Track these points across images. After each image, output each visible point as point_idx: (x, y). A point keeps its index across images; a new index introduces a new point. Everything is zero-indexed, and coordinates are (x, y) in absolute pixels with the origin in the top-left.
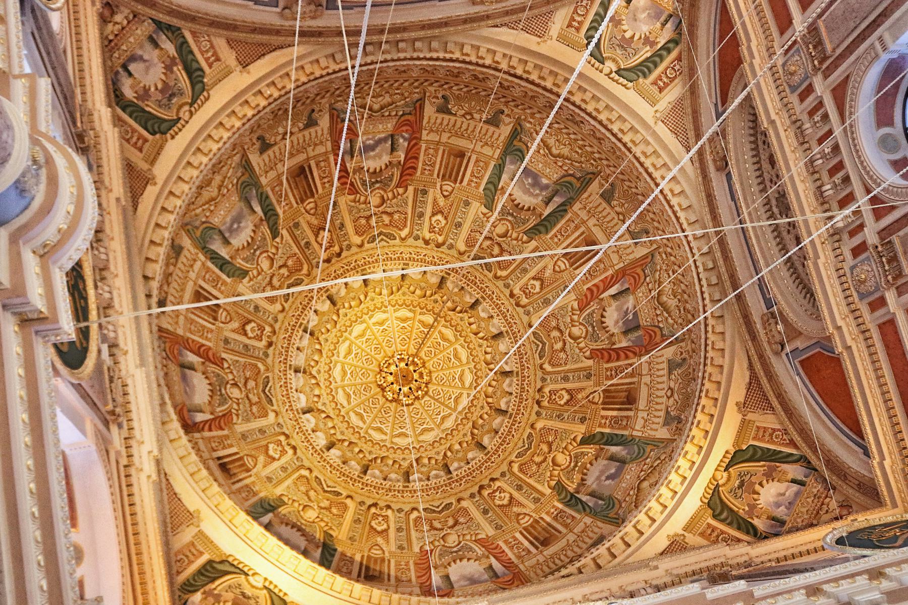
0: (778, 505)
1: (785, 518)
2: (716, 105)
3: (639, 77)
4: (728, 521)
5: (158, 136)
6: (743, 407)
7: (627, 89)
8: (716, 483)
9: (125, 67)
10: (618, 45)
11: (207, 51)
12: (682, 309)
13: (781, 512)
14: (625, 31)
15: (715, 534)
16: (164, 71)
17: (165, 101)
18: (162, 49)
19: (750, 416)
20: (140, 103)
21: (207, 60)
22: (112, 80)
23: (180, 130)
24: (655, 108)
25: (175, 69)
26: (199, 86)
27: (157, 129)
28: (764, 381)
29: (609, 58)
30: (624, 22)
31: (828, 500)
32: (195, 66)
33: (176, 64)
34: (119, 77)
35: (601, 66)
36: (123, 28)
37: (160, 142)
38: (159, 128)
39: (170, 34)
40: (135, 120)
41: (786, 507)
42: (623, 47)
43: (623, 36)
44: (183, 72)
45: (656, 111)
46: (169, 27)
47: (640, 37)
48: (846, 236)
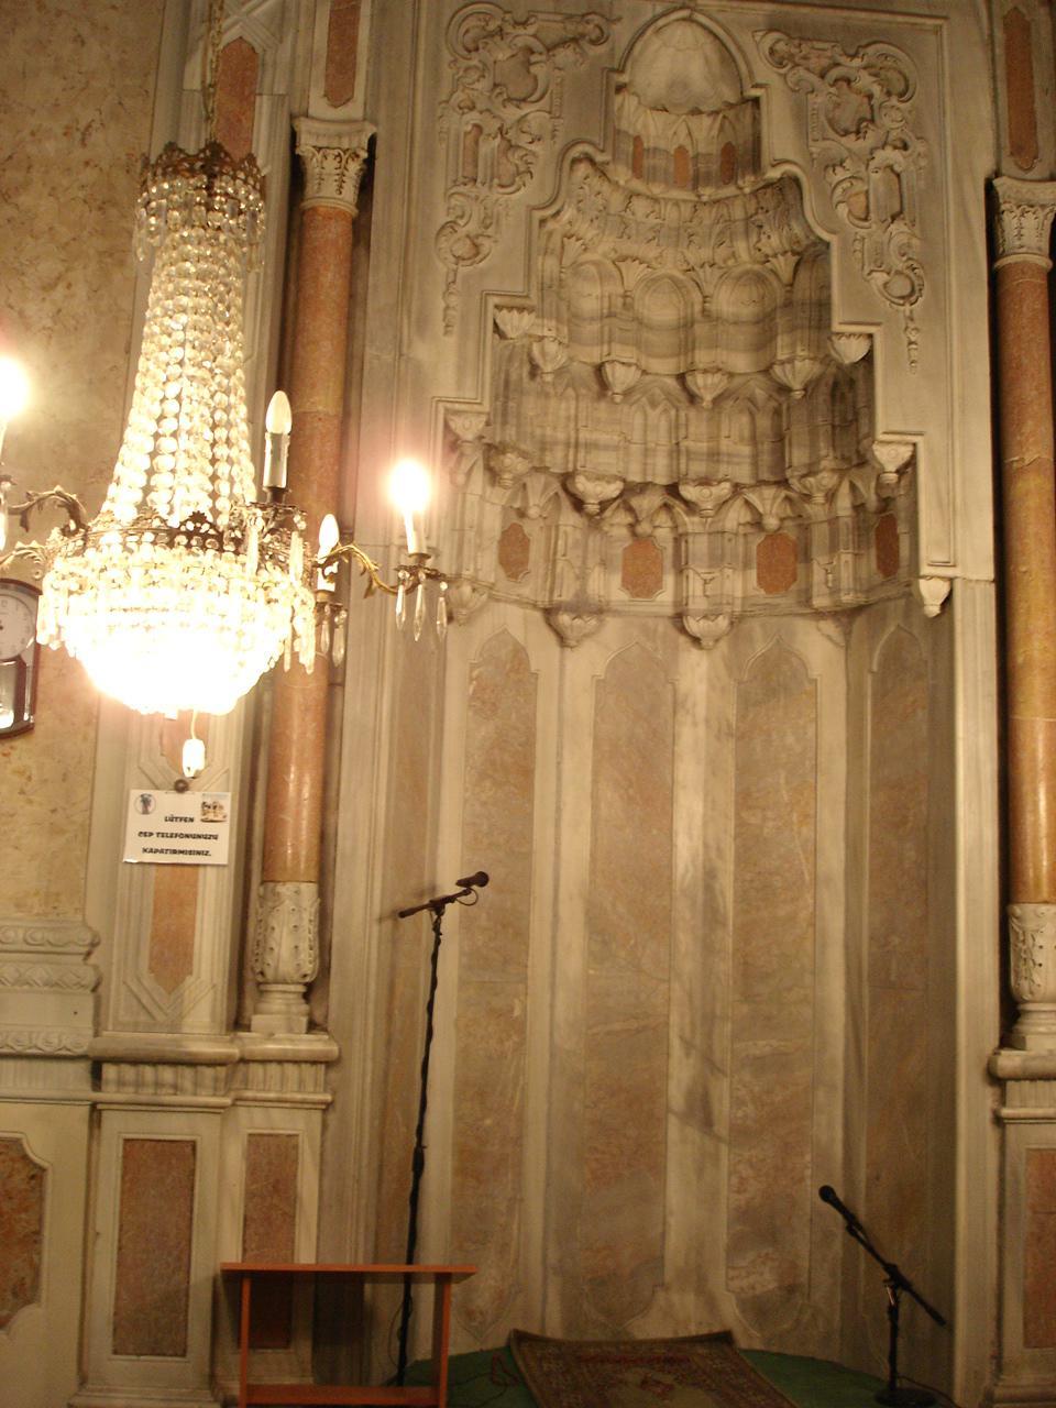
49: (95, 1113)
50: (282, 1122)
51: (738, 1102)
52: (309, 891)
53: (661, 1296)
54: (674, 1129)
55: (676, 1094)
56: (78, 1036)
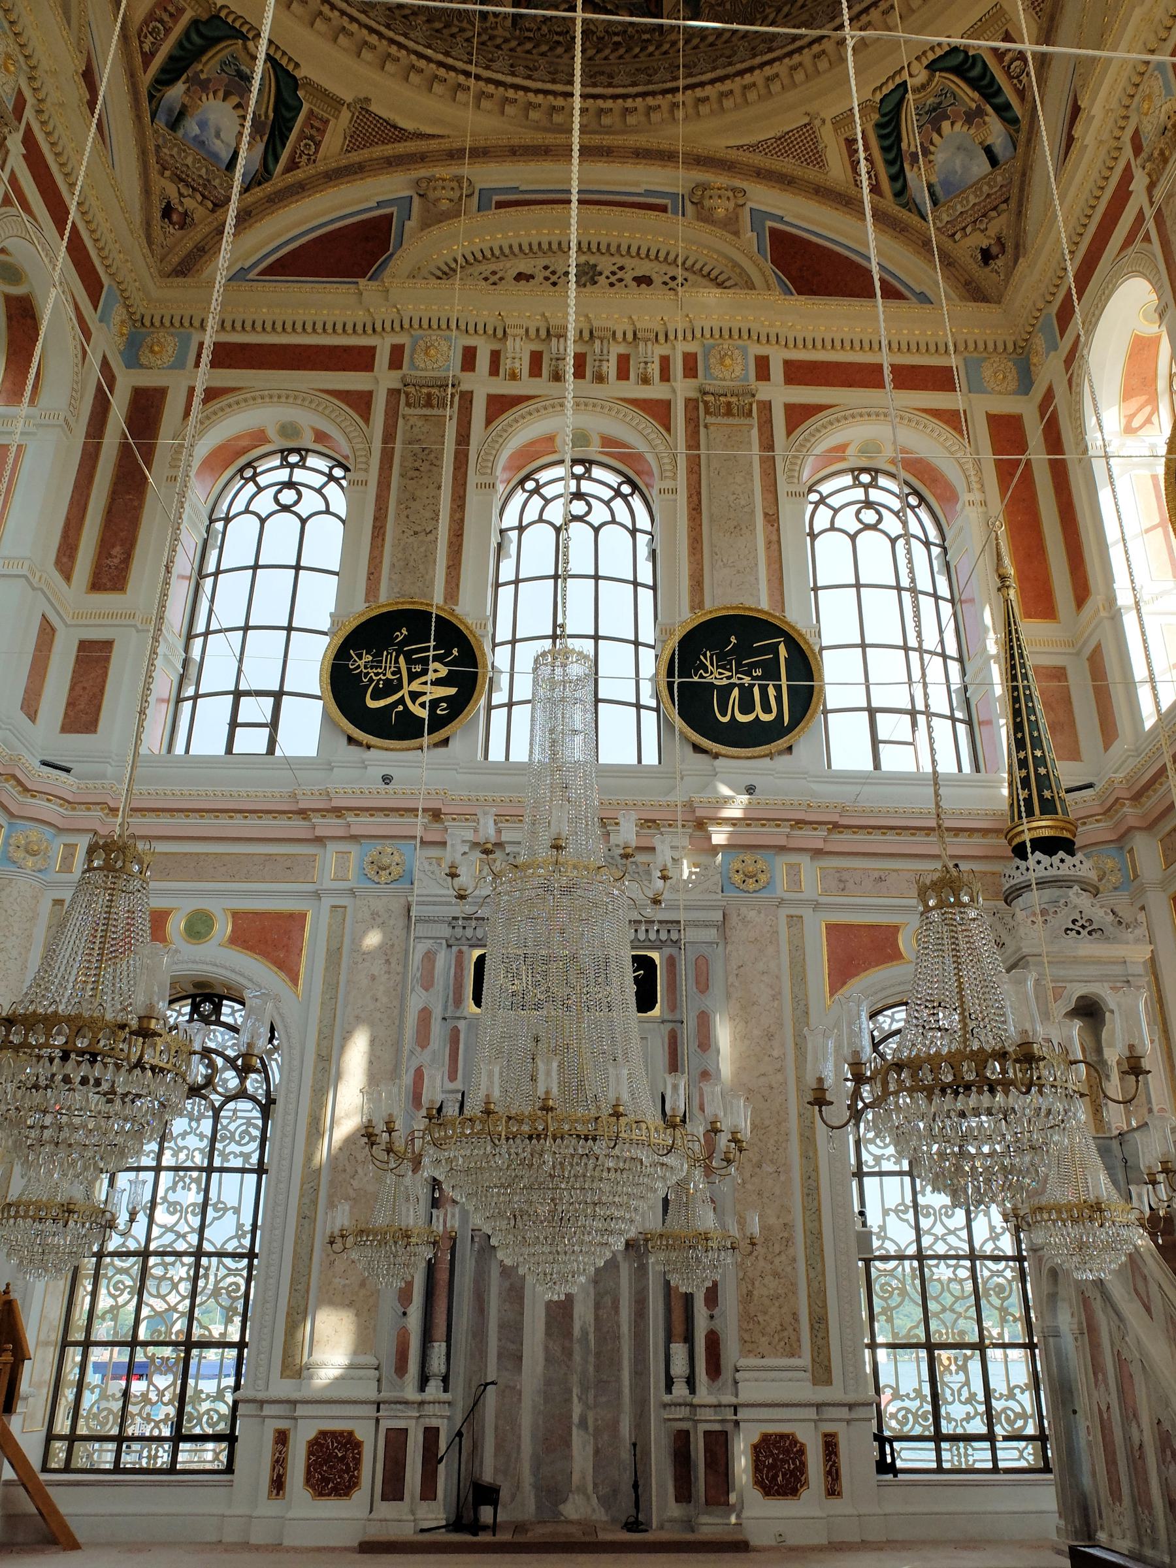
0: (202, 125)
1: (180, 133)
2: (781, 219)
3: (883, 116)
4: (186, 44)
6: (362, 107)
7: (875, 90)
8: (250, 36)
10: (940, 103)
12: (561, 39)
13: (191, 127)
14: (953, 124)
15: (166, 18)
19: (345, 115)
24: (828, 122)
28: (389, 150)
29: (930, 80)
30: (965, 128)
31: (199, 198)
35: (925, 62)
41: (196, 136)
42: (935, 110)
43: (948, 118)
45: (824, 121)
47: (932, 143)
48: (496, 347)
49: (377, 1420)
50: (434, 1423)
51: (596, 1420)
52: (444, 1344)
53: (570, 1496)
54: (575, 1431)
55: (576, 1419)
56: (372, 1394)
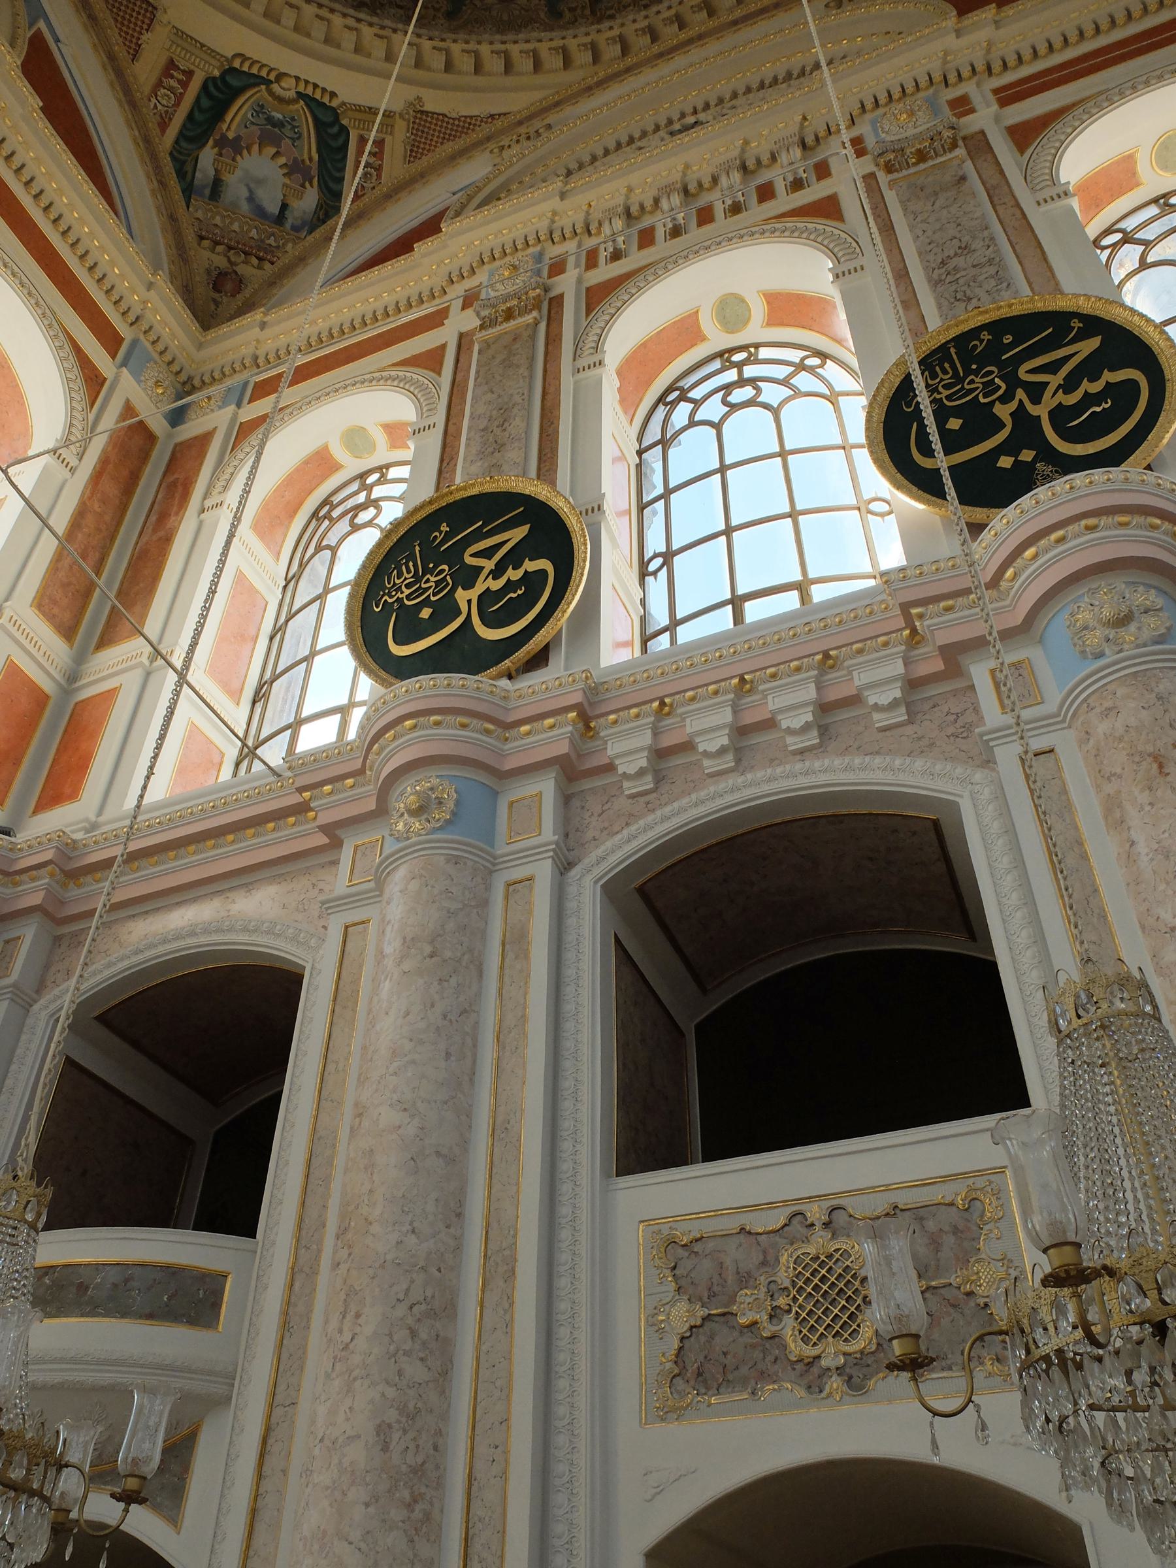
5: (345, 122)
9: (280, 219)
11: (171, 89)
16: (245, 152)
17: (287, 130)
18: (216, 170)
20: (314, 172)
21: (185, 85)
22: (310, 232)
23: (315, 86)
25: (231, 135)
26: (234, 82)
27: (335, 129)
32: (206, 103)
33: (224, 137)
34: (299, 222)
36: (230, 248)
37: (350, 113)
38: (332, 125)
39: (188, 168)
40: (343, 169)
44: (228, 118)
46: (181, 174)
